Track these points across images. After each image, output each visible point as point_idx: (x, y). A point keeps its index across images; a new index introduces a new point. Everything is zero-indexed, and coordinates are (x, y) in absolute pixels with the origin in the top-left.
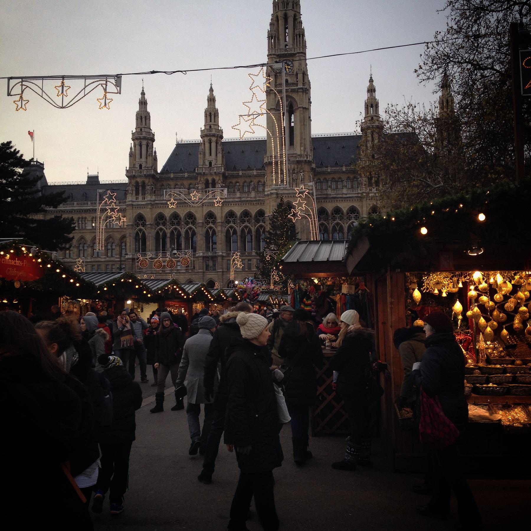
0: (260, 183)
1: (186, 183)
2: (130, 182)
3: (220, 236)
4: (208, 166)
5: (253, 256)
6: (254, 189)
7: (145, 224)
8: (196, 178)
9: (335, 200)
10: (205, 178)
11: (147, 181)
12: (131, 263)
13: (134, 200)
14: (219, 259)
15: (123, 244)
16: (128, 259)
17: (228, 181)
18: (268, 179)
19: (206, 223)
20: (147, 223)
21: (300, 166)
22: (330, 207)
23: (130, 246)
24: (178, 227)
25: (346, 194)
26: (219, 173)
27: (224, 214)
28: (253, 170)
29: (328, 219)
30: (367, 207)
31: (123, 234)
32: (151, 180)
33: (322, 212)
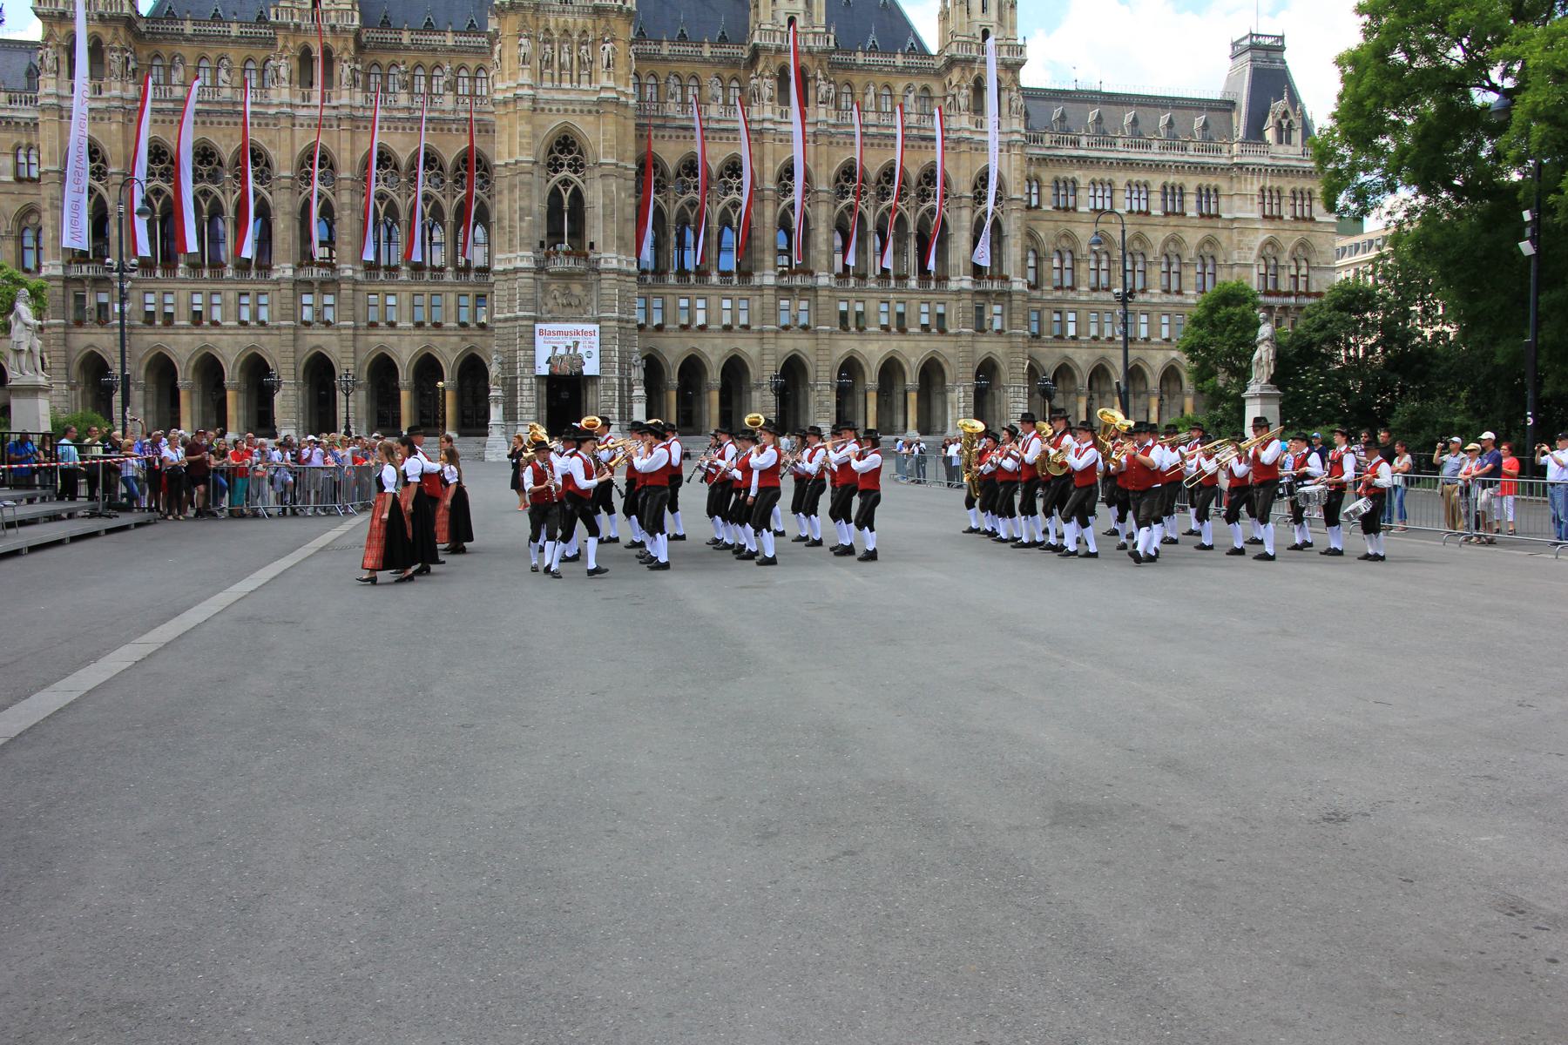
0: (463, 73)
1: (235, 54)
3: (346, 220)
4: (309, 6)
5: (446, 284)
6: (452, 86)
7: (105, 174)
8: (270, 43)
9: (688, 134)
10: (300, 41)
15: (29, 234)
16: (48, 278)
18: (506, 55)
19: (302, 178)
20: (111, 170)
21: (603, 23)
22: (670, 153)
24: (212, 187)
25: (719, 121)
26: (344, 30)
28: (443, 32)
29: (664, 187)
30: (775, 163)
31: (27, 200)
33: (647, 166)
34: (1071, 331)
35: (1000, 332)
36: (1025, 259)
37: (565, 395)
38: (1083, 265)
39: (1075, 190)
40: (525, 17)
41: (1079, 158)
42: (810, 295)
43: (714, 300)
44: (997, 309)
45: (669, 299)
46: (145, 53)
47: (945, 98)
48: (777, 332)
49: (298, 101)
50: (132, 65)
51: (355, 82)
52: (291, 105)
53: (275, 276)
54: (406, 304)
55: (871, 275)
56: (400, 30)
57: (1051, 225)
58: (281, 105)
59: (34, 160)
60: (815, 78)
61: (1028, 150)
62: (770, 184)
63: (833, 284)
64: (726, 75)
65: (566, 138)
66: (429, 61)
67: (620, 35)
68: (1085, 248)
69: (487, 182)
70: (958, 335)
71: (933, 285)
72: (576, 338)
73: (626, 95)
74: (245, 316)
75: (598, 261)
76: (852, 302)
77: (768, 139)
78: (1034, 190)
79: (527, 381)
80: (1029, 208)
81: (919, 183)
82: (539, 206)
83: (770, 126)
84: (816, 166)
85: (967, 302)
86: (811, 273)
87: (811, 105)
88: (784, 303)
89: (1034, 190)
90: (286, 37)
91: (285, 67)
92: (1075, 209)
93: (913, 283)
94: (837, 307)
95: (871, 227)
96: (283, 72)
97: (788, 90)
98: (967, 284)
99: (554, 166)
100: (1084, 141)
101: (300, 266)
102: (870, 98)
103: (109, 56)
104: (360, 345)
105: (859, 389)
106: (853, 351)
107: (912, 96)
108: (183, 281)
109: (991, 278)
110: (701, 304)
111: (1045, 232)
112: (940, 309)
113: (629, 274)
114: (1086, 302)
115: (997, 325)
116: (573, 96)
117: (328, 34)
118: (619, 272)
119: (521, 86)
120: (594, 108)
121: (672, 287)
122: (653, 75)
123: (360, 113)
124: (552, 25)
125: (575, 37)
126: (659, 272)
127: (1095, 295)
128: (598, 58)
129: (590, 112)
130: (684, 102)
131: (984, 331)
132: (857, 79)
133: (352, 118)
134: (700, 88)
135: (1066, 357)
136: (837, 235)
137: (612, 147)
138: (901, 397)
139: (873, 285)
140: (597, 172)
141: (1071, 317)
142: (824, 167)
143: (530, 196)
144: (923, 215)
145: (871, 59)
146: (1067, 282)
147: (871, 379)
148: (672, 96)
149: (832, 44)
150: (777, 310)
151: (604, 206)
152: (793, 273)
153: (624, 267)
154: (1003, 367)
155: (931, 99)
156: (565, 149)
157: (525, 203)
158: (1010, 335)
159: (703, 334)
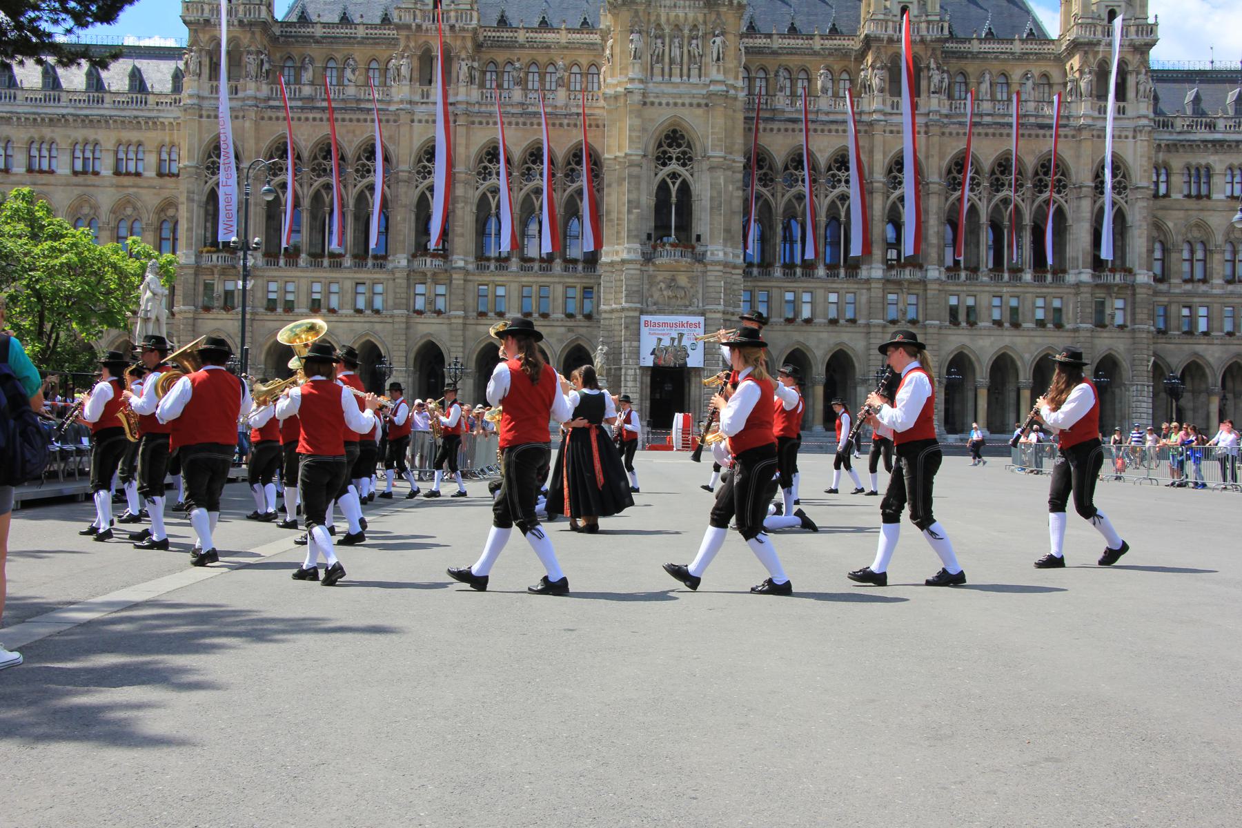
0: (575, 69)
2: (194, 41)
3: (459, 213)
4: (431, 6)
11: (245, 39)
12: (191, 281)
13: (206, 93)
14: (458, 278)
15: (167, 227)
17: (486, 56)
18: (617, 50)
19: (418, 172)
23: (190, 229)
25: (827, 113)
27: (474, 150)
29: (772, 180)
30: (884, 154)
31: (166, 193)
32: (258, 36)
34: (1202, 326)
35: (1122, 327)
36: (1151, 251)
37: (668, 387)
38: (1217, 257)
39: (1209, 176)
40: (636, 12)
41: (1214, 142)
42: (919, 289)
43: (820, 293)
44: (1119, 303)
45: (775, 293)
46: (278, 55)
47: (1065, 84)
48: (884, 326)
49: (417, 98)
50: (266, 66)
51: (471, 79)
52: (411, 102)
53: (390, 266)
54: (515, 295)
55: (983, 268)
56: (516, 30)
57: (1181, 214)
58: (402, 102)
59: (174, 157)
60: (928, 68)
61: (1156, 136)
62: (879, 176)
63: (943, 277)
64: (836, 67)
65: (674, 131)
66: (542, 57)
67: (731, 28)
68: (1219, 238)
69: (597, 176)
70: (1076, 330)
71: (1049, 277)
72: (681, 330)
73: (735, 88)
74: (361, 303)
75: (704, 254)
76: (962, 296)
77: (878, 129)
78: (1163, 178)
79: (631, 372)
80: (1156, 196)
81: (1036, 174)
82: (648, 200)
83: (882, 118)
84: (927, 157)
85: (1086, 295)
86: (921, 267)
87: (924, 96)
88: (891, 297)
89: (1163, 178)
90: (408, 37)
91: (405, 65)
92: (1208, 197)
93: (1028, 276)
94: (947, 301)
95: (984, 218)
96: (404, 71)
97: (899, 82)
98: (1086, 276)
99: (663, 160)
100: (1221, 124)
101: (414, 256)
102: (985, 87)
103: (245, 59)
104: (470, 333)
105: (969, 386)
106: (963, 346)
107: (1030, 83)
108: (304, 269)
109: (1113, 270)
110: (806, 297)
111: (1173, 222)
112: (1057, 303)
113: (735, 267)
114: (1220, 296)
115: (1119, 320)
116: (683, 89)
117: (448, 33)
118: (726, 264)
119: (632, 80)
120: (703, 102)
121: (778, 279)
122: (764, 69)
123: (476, 108)
124: (663, 20)
125: (686, 32)
126: (765, 265)
127: (1230, 288)
128: (708, 51)
129: (699, 105)
130: (793, 94)
131: (1103, 326)
132: (972, 68)
133: (467, 114)
134: (809, 80)
135: (1196, 354)
136: (948, 229)
137: (720, 140)
138: (1013, 395)
139: (985, 279)
140: (705, 165)
141: (1202, 311)
142: (936, 159)
143: (638, 189)
144: (1040, 206)
145: (986, 47)
146: (1198, 274)
147: (982, 376)
148: (782, 89)
149: (946, 32)
150: (885, 304)
151: (712, 199)
152: (904, 266)
153: (730, 258)
154: (1125, 364)
155: (1050, 85)
156: (673, 144)
157: (634, 196)
158: (1133, 331)
159: (809, 328)
